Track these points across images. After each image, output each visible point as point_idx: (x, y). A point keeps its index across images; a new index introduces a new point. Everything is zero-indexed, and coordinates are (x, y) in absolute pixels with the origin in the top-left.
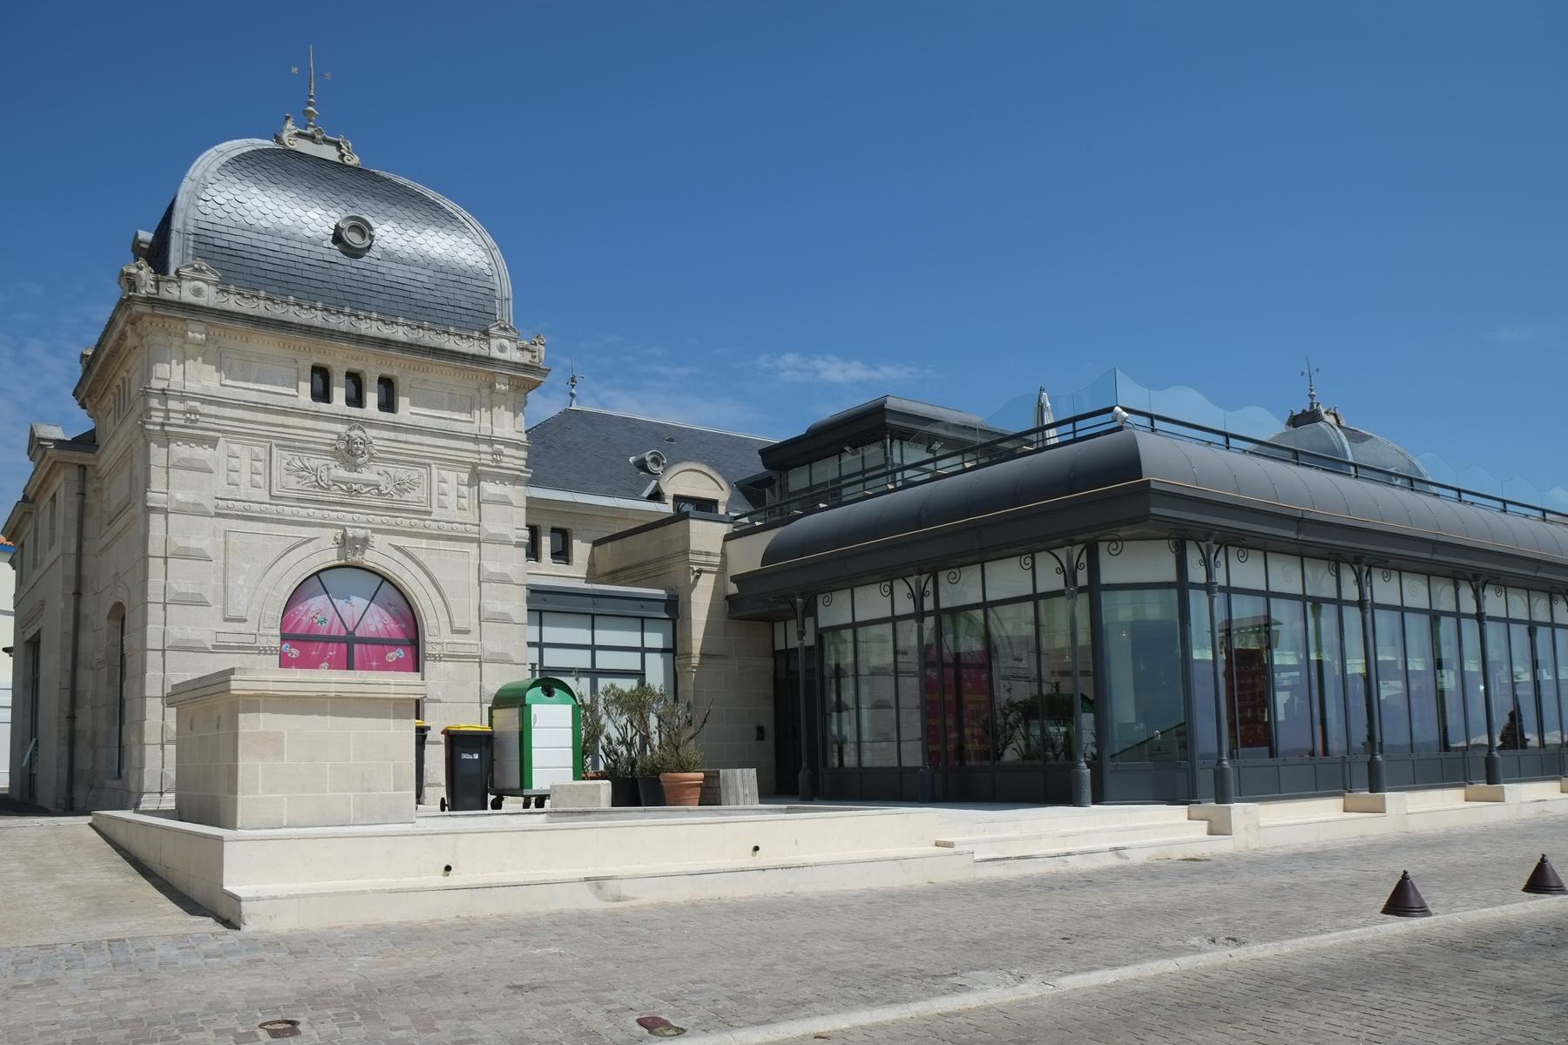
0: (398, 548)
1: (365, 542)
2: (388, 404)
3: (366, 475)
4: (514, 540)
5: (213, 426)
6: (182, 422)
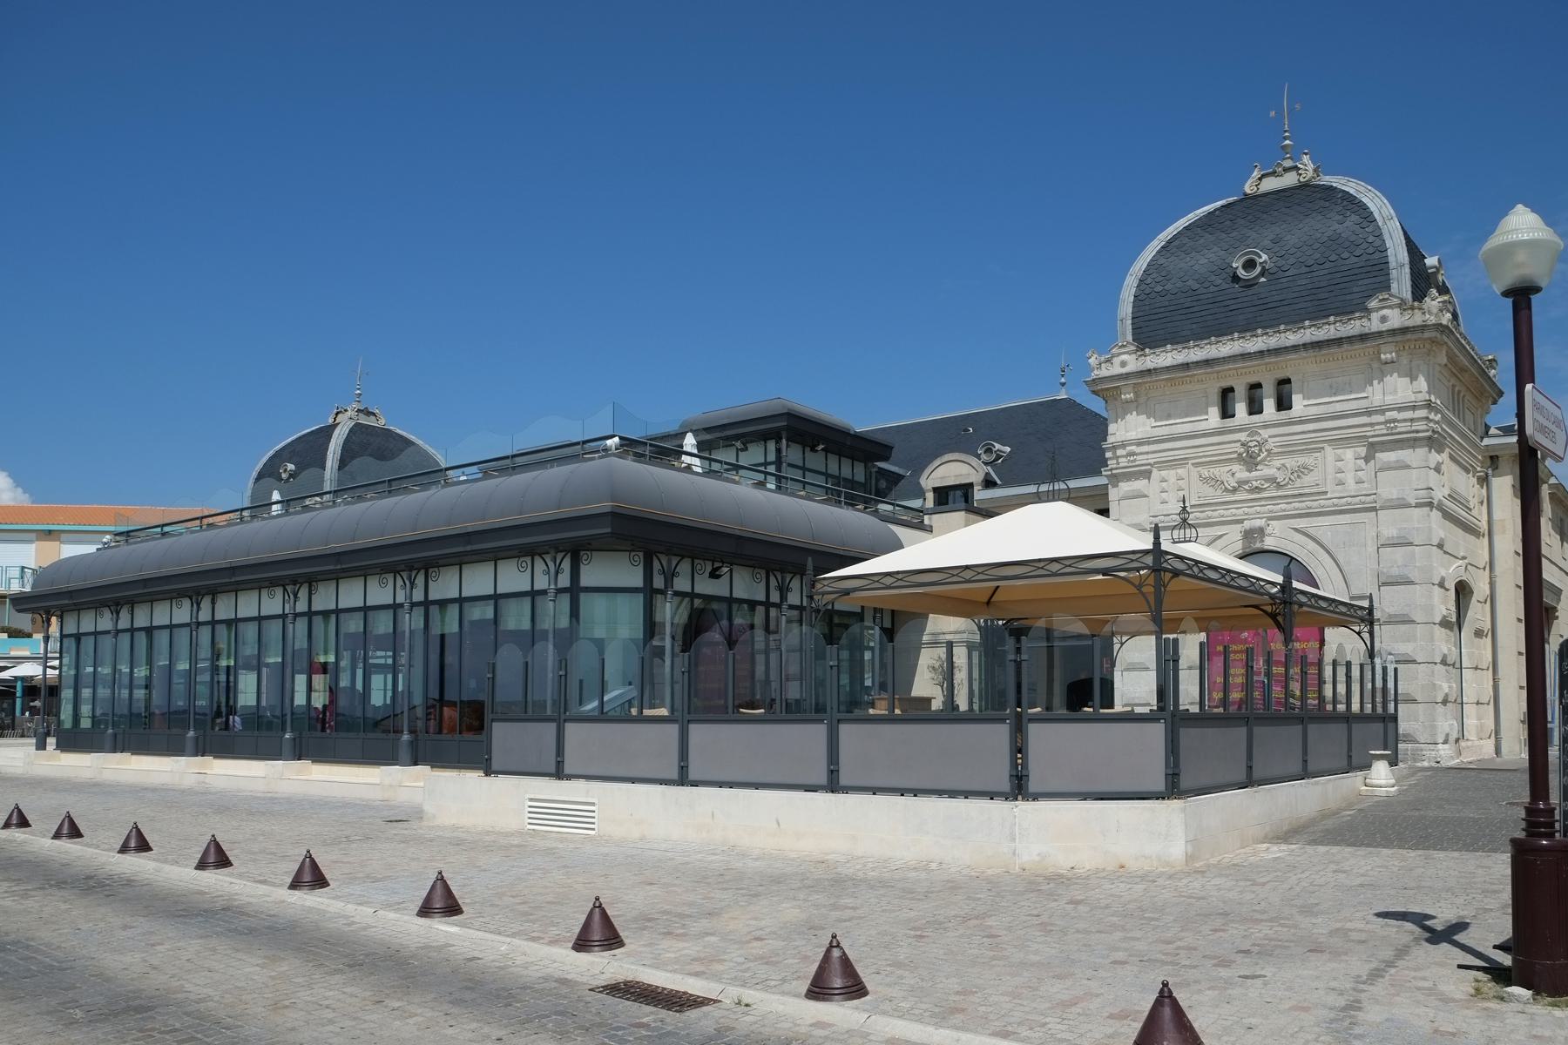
0: (1296, 530)
1: (1261, 531)
2: (1283, 404)
3: (1266, 471)
4: (1413, 502)
5: (1226, 451)
6: (1385, 432)
